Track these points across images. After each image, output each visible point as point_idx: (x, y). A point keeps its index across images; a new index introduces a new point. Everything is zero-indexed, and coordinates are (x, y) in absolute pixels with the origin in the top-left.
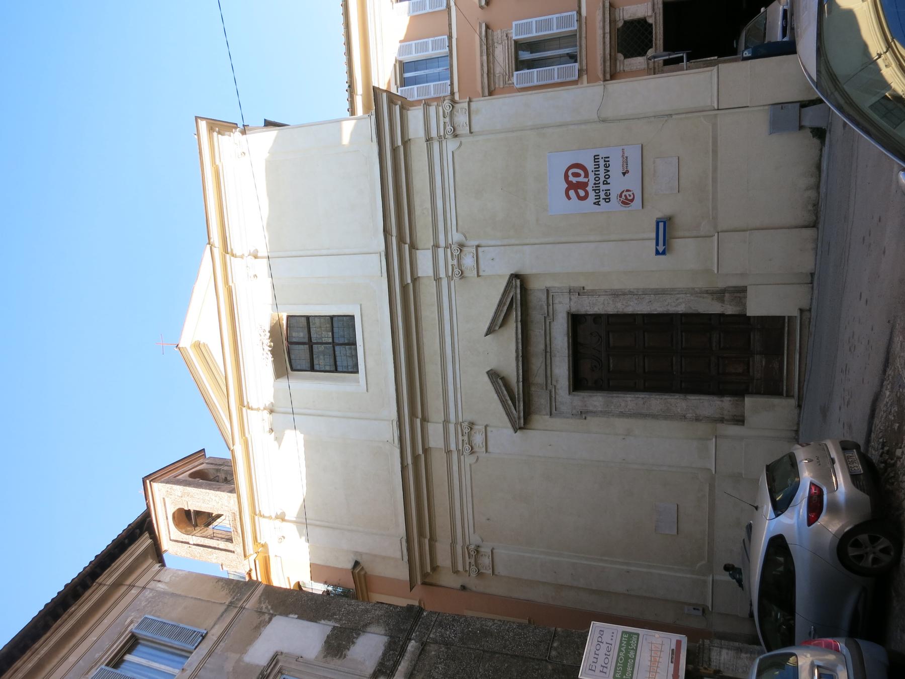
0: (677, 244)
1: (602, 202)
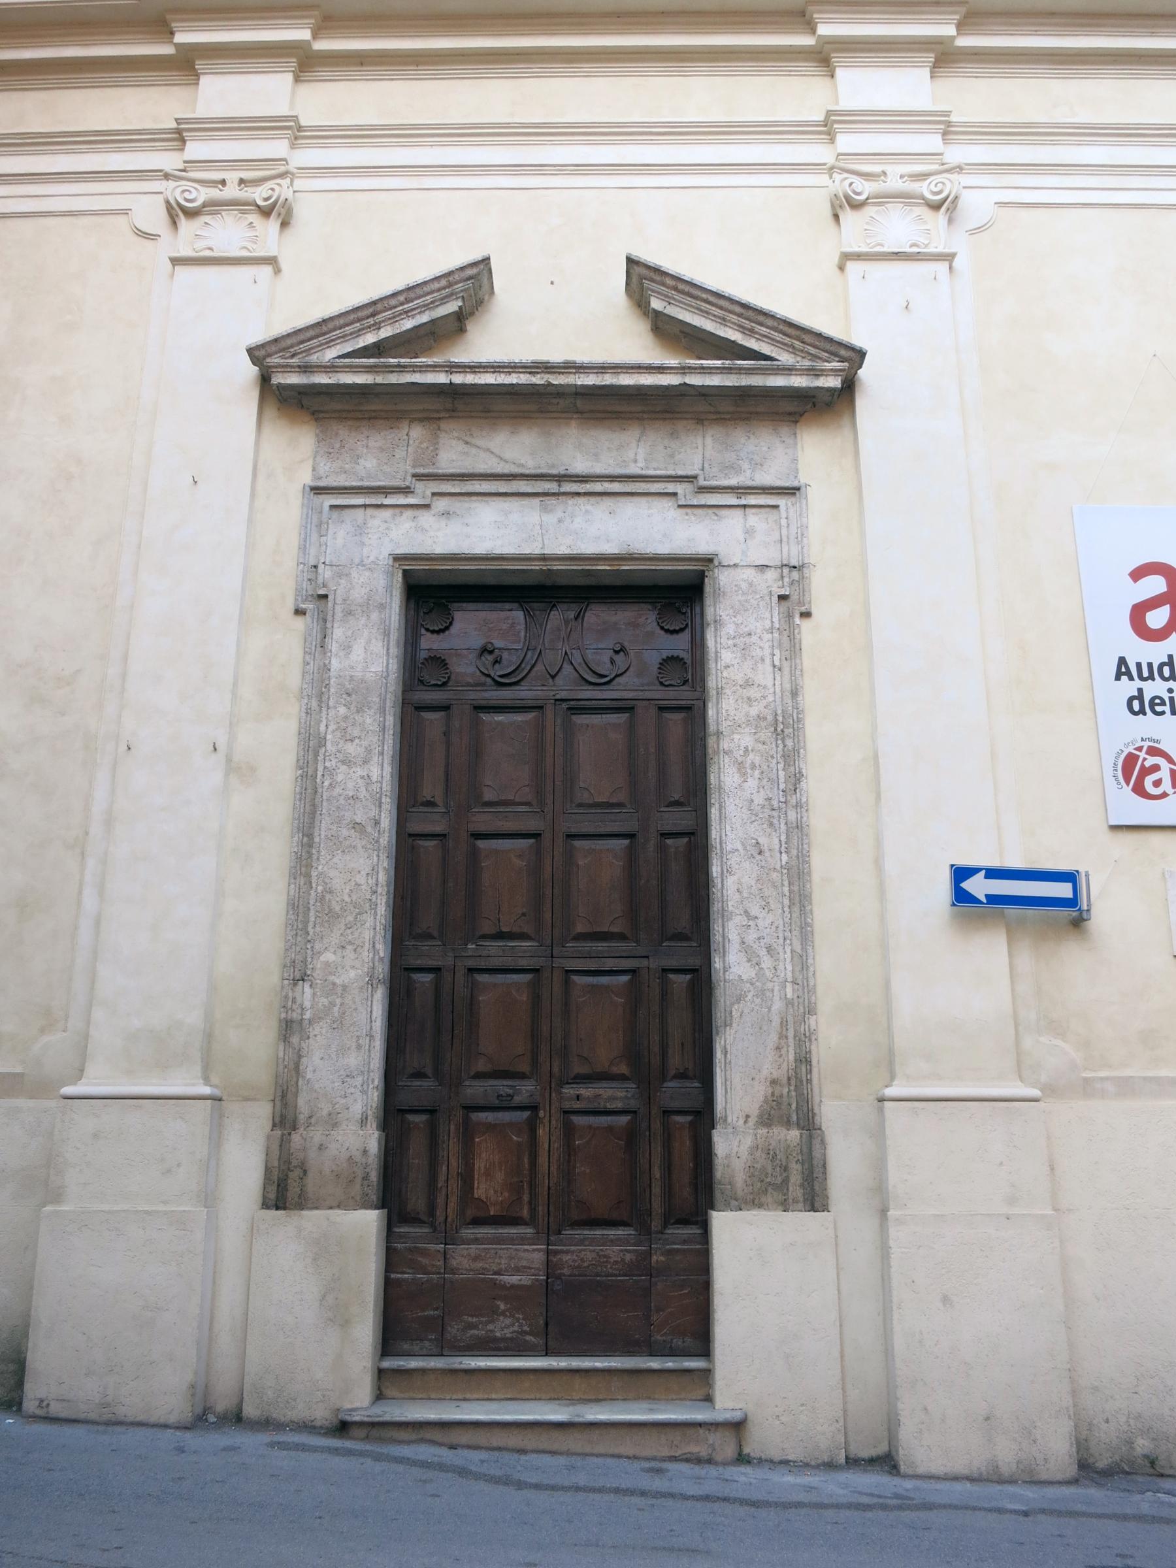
0: (991, 951)
1: (1129, 687)
